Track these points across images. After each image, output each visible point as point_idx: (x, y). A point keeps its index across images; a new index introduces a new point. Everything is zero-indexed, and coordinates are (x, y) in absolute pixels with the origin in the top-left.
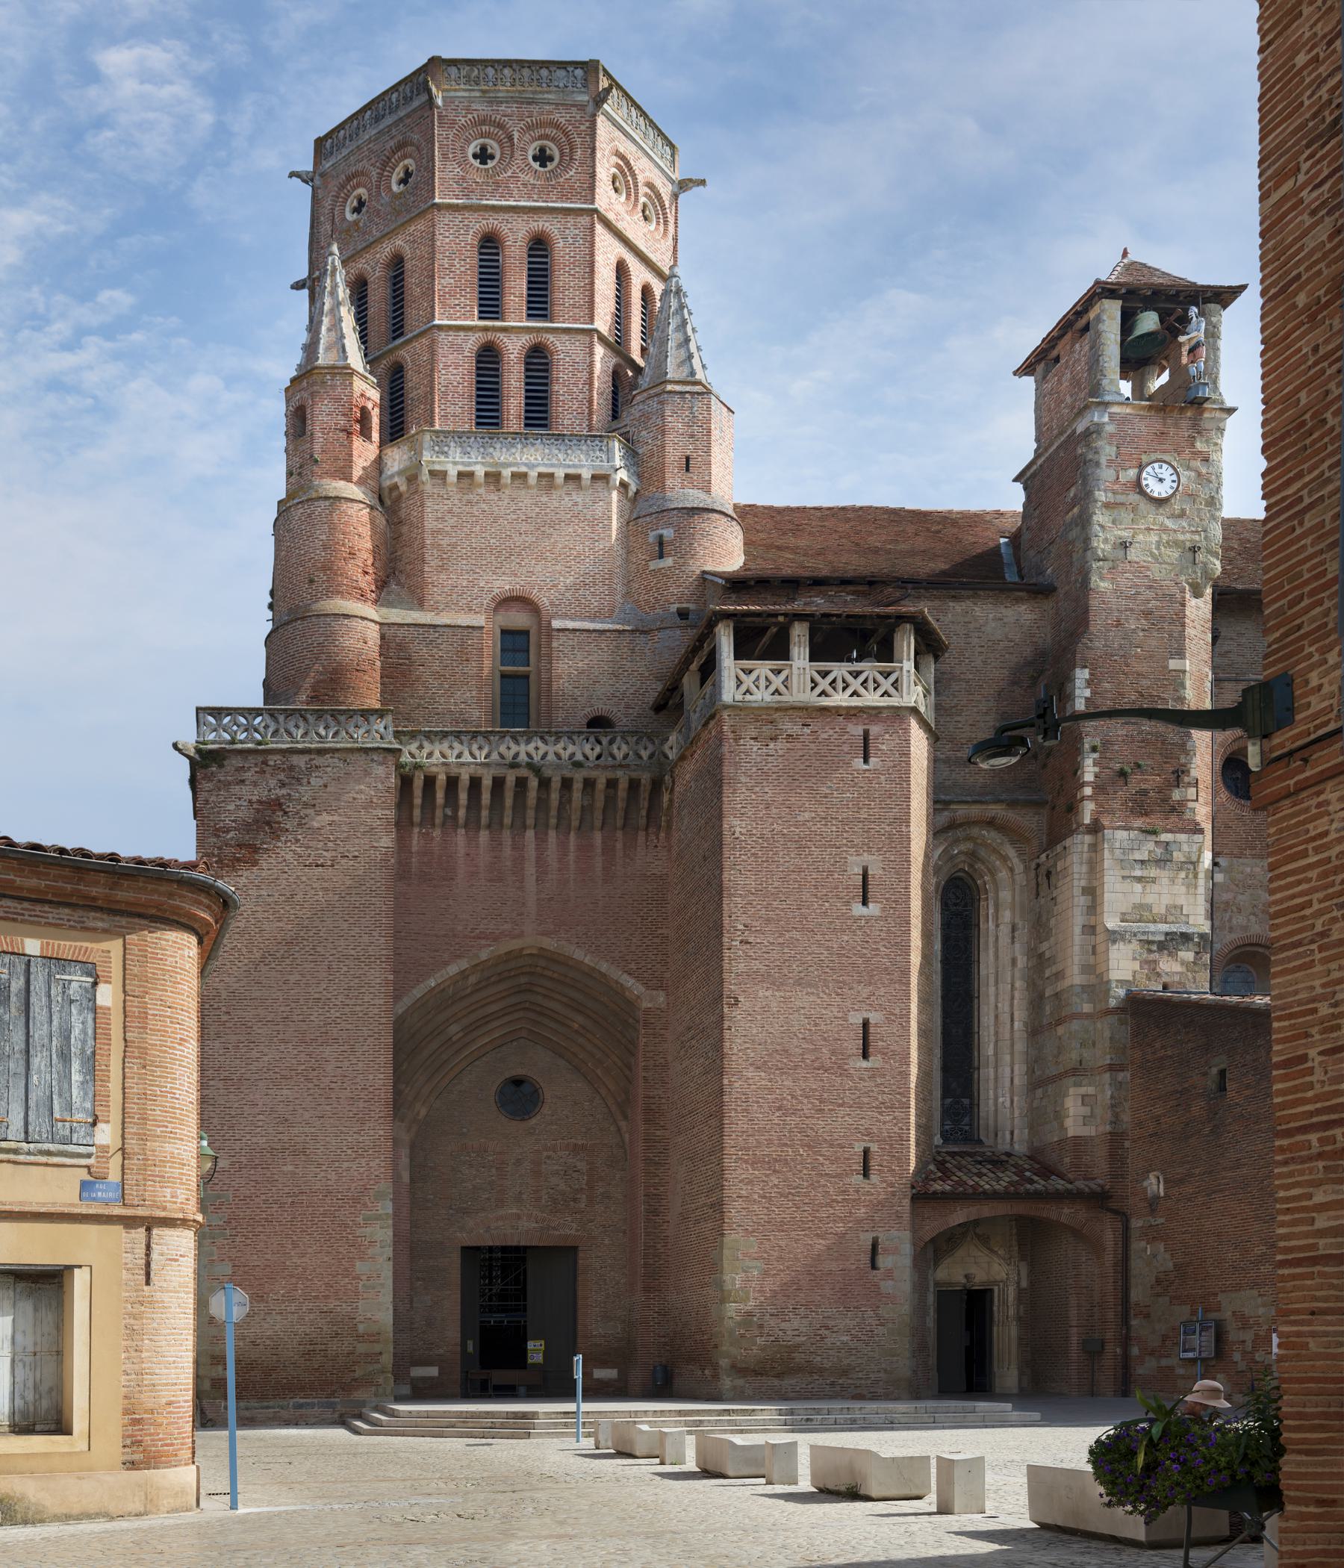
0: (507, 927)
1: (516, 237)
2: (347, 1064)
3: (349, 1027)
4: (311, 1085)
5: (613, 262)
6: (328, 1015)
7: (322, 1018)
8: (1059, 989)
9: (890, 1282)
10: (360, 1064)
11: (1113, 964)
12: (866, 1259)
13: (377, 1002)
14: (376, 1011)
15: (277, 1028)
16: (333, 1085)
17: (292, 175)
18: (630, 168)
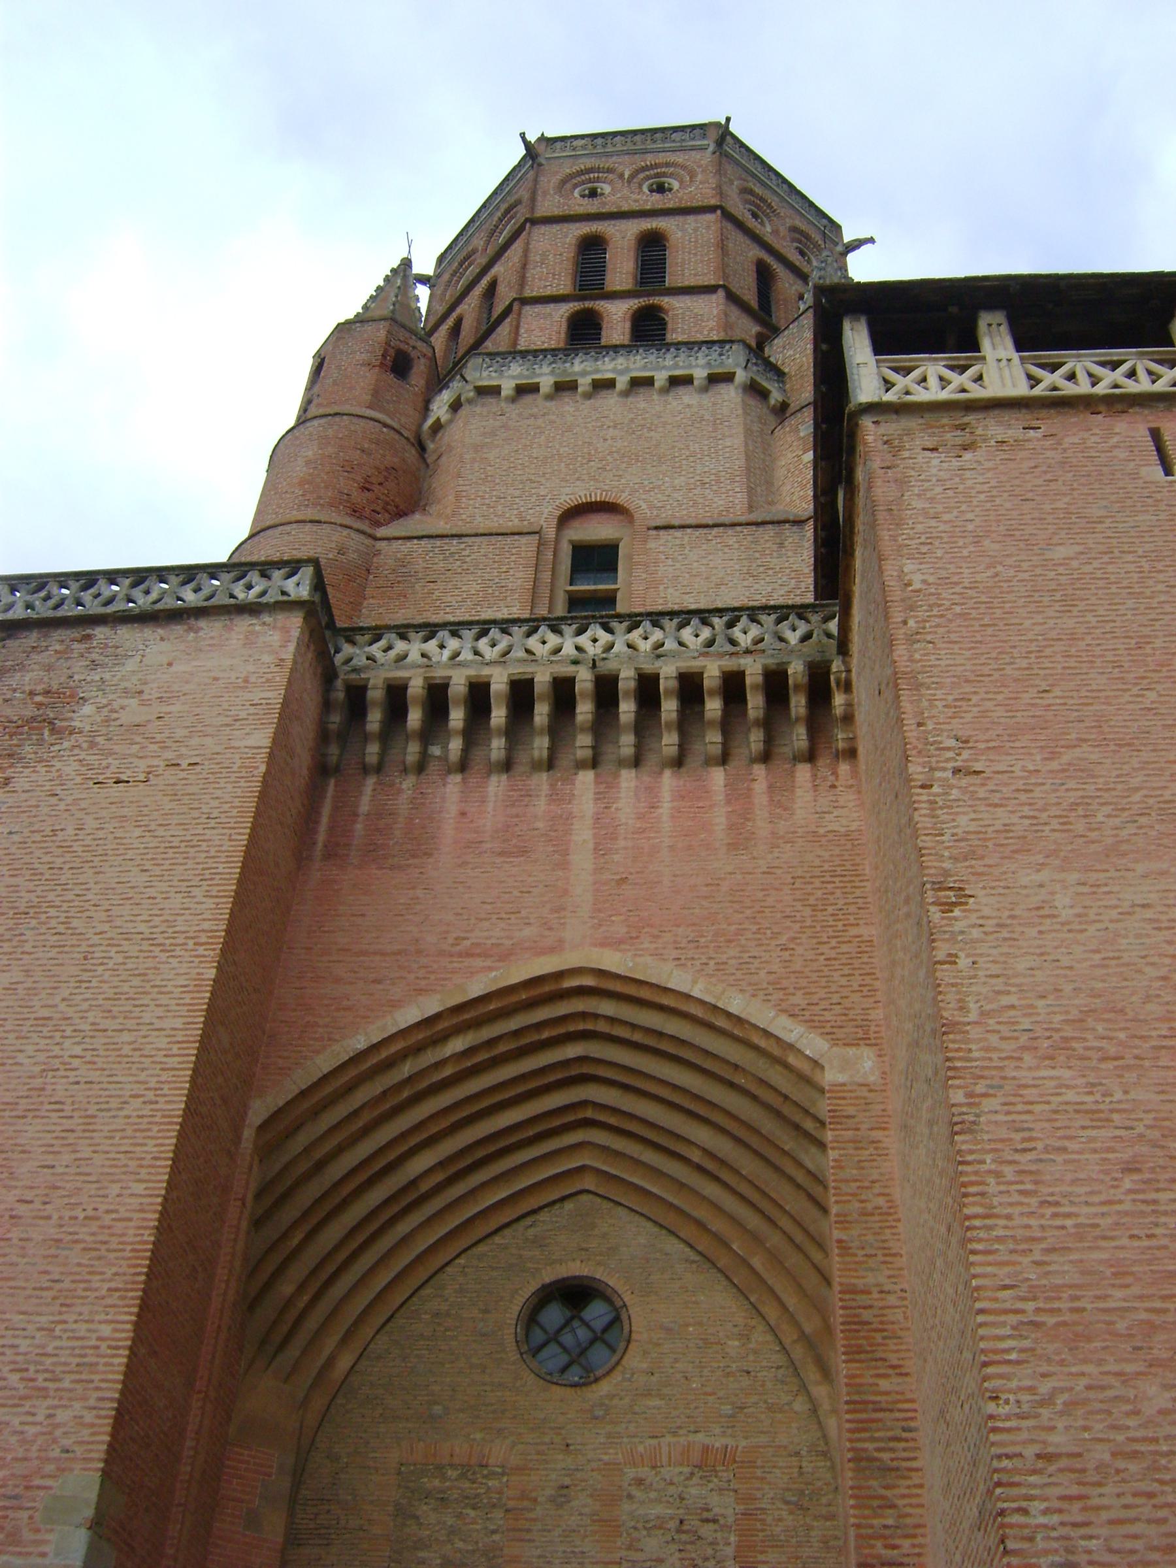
0: (527, 932)
2: (66, 1158)
3: (95, 1076)
6: (57, 1051)
7: (42, 1057)
10: (98, 1159)
13: (168, 1024)
14: (162, 1042)
16: (22, 1209)
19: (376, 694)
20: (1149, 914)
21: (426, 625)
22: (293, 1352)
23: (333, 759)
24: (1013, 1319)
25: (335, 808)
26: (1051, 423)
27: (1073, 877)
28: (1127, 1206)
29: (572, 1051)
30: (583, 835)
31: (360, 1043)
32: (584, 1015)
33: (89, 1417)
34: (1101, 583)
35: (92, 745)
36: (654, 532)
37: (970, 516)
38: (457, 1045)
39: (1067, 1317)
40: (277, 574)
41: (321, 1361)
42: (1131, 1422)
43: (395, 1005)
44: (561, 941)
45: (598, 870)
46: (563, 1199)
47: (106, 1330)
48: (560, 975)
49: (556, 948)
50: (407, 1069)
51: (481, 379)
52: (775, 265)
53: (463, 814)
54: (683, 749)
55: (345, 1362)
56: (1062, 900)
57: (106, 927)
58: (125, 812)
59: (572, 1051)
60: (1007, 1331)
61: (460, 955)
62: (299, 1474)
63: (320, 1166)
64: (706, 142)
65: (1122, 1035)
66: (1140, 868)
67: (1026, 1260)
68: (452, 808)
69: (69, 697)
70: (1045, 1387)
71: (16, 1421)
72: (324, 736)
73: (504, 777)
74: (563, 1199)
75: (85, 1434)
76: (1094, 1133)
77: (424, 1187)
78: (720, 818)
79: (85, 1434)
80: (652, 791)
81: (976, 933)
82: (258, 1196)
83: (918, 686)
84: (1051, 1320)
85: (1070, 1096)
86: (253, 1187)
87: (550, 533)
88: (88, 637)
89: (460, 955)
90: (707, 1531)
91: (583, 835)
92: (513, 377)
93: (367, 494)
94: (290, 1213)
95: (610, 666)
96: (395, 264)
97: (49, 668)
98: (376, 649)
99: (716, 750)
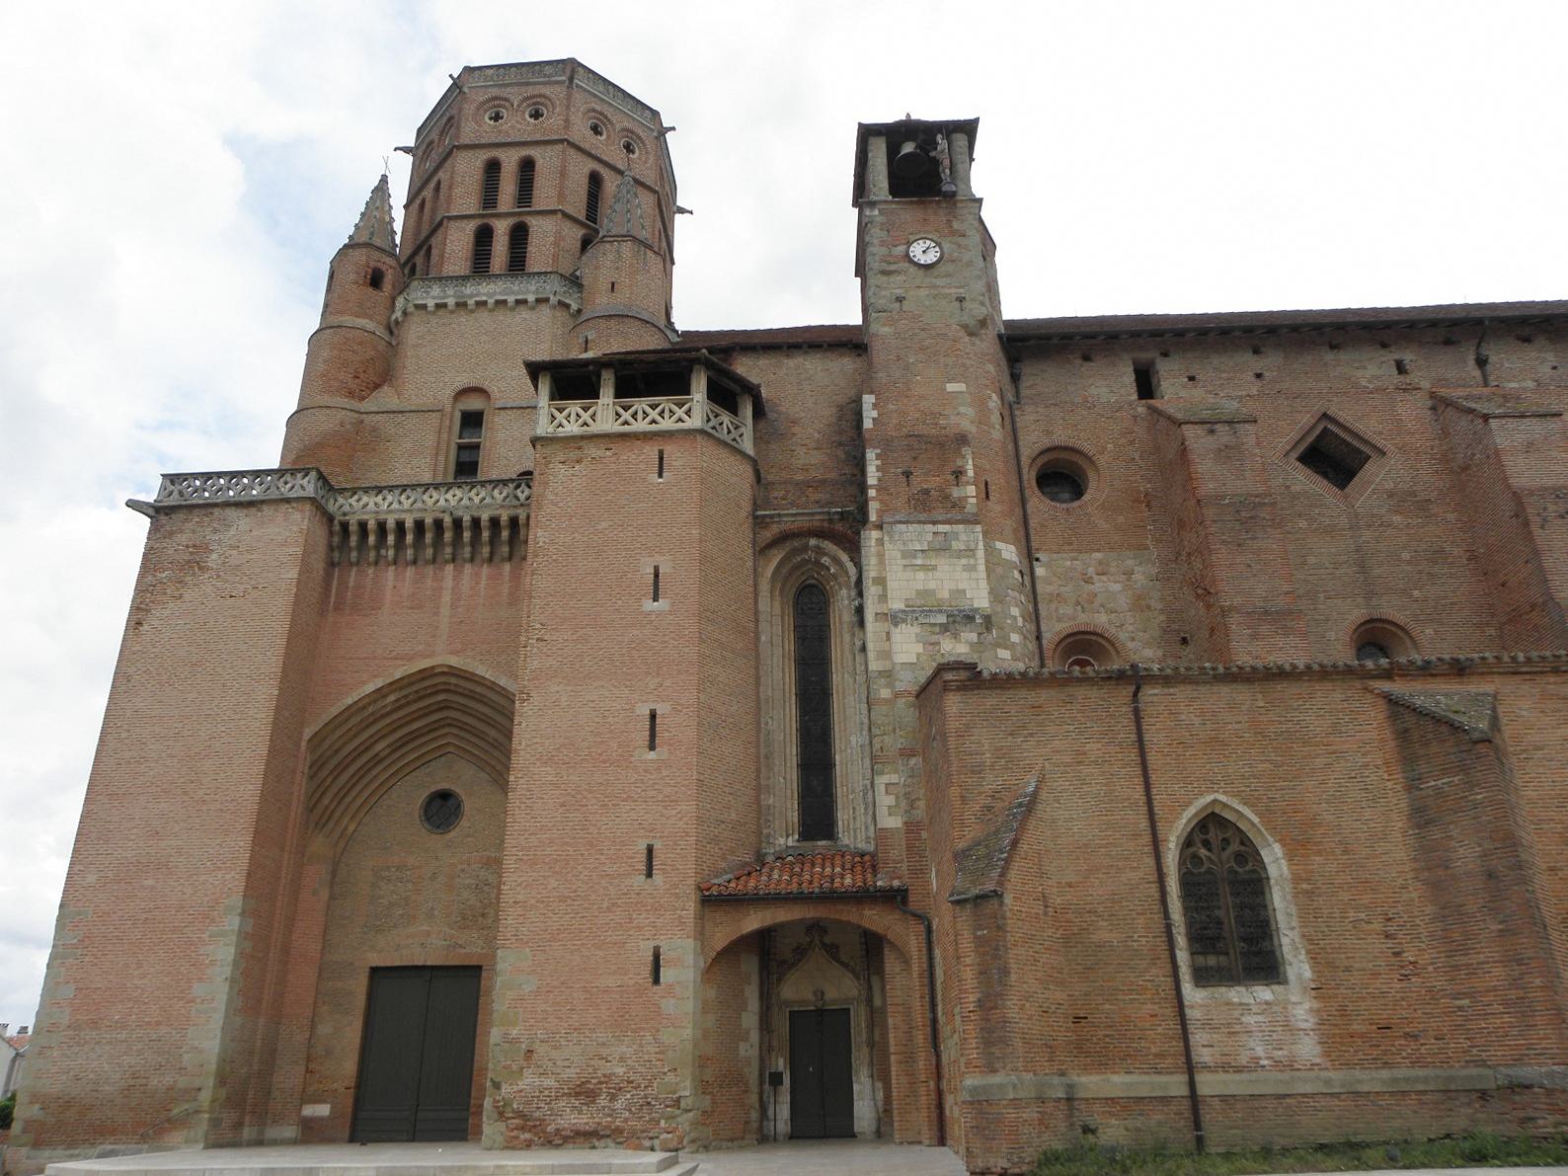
1: (510, 160)
4: (186, 798)
5: (586, 171)
7: (209, 732)
9: (672, 1001)
10: (234, 776)
12: (646, 971)
15: (167, 743)
17: (396, 149)
18: (606, 117)
19: (353, 528)
20: (592, 705)
21: (376, 487)
22: (331, 825)
23: (336, 560)
24: (514, 858)
25: (339, 584)
26: (616, 447)
27: (570, 688)
28: (558, 819)
29: (441, 697)
30: (446, 598)
31: (350, 701)
32: (445, 683)
33: (237, 876)
34: (615, 543)
35: (218, 576)
36: (497, 411)
37: (570, 504)
38: (392, 698)
39: (532, 857)
40: (299, 475)
41: (344, 825)
42: (544, 891)
43: (364, 683)
44: (434, 652)
45: (451, 617)
46: (440, 756)
47: (242, 844)
48: (433, 668)
49: (432, 655)
50: (371, 709)
51: (416, 299)
52: (604, 172)
53: (395, 587)
54: (492, 553)
55: (351, 828)
56: (564, 699)
57: (230, 671)
58: (235, 613)
59: (441, 697)
60: (512, 862)
61: (391, 659)
62: (334, 873)
63: (337, 751)
64: (564, 78)
65: (572, 755)
66: (595, 684)
67: (522, 838)
68: (390, 584)
69: (204, 548)
70: (520, 880)
71: (210, 879)
72: (331, 548)
73: (413, 568)
74: (440, 756)
75: (236, 883)
76: (554, 792)
77: (382, 755)
78: (505, 590)
79: (236, 883)
80: (478, 575)
81: (530, 713)
82: (311, 767)
83: (531, 597)
84: (526, 858)
85: (550, 778)
86: (308, 764)
87: (448, 408)
88: (211, 513)
89: (391, 659)
90: (486, 888)
91: (446, 598)
92: (434, 298)
93: (357, 380)
94: (325, 772)
95: (460, 513)
96: (380, 178)
97: (194, 532)
98: (353, 501)
99: (506, 555)
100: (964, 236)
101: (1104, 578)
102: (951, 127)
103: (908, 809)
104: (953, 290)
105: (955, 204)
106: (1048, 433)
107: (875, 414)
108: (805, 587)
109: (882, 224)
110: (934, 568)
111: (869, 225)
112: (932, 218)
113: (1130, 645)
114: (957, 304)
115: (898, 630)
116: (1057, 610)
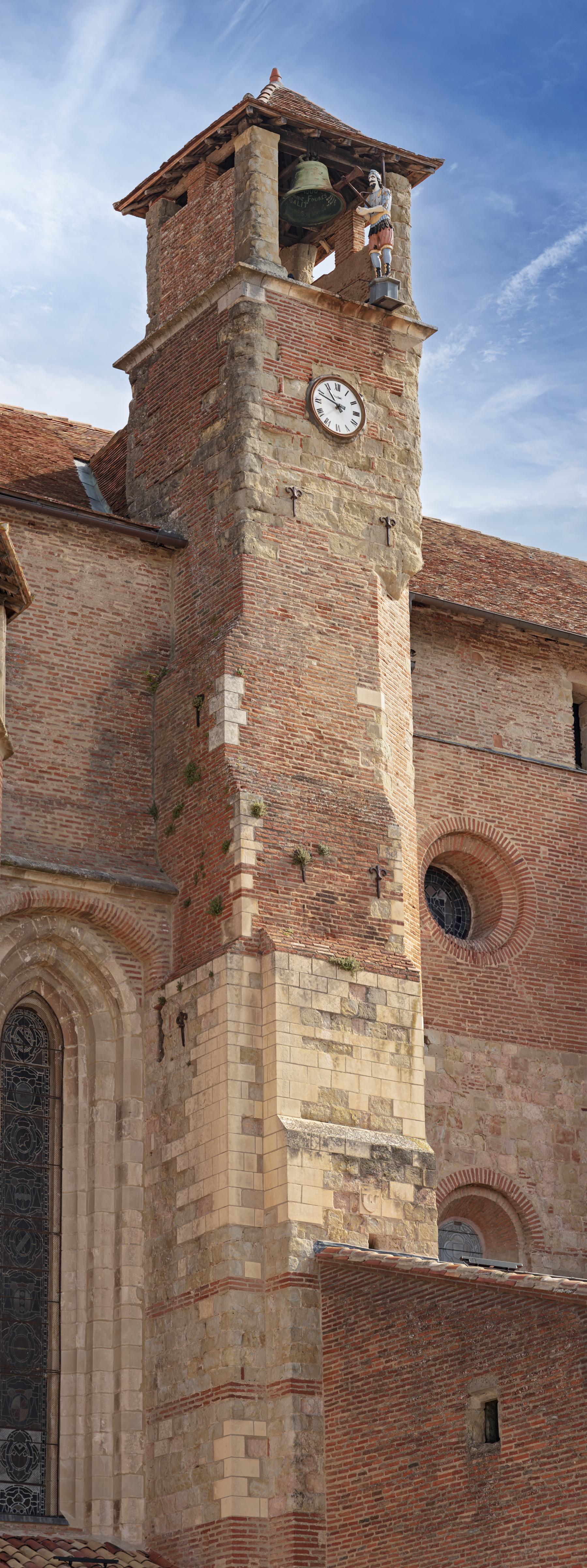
8: (202, 1230)
11: (293, 1192)
100: (400, 395)
101: (518, 1091)
102: (394, 160)
103: (300, 1487)
104: (377, 501)
105: (390, 323)
106: (457, 802)
107: (242, 717)
108: (19, 1008)
109: (270, 324)
110: (349, 1051)
111: (246, 319)
112: (352, 340)
113: (545, 1220)
114: (381, 529)
115: (297, 1161)
116: (447, 1138)
